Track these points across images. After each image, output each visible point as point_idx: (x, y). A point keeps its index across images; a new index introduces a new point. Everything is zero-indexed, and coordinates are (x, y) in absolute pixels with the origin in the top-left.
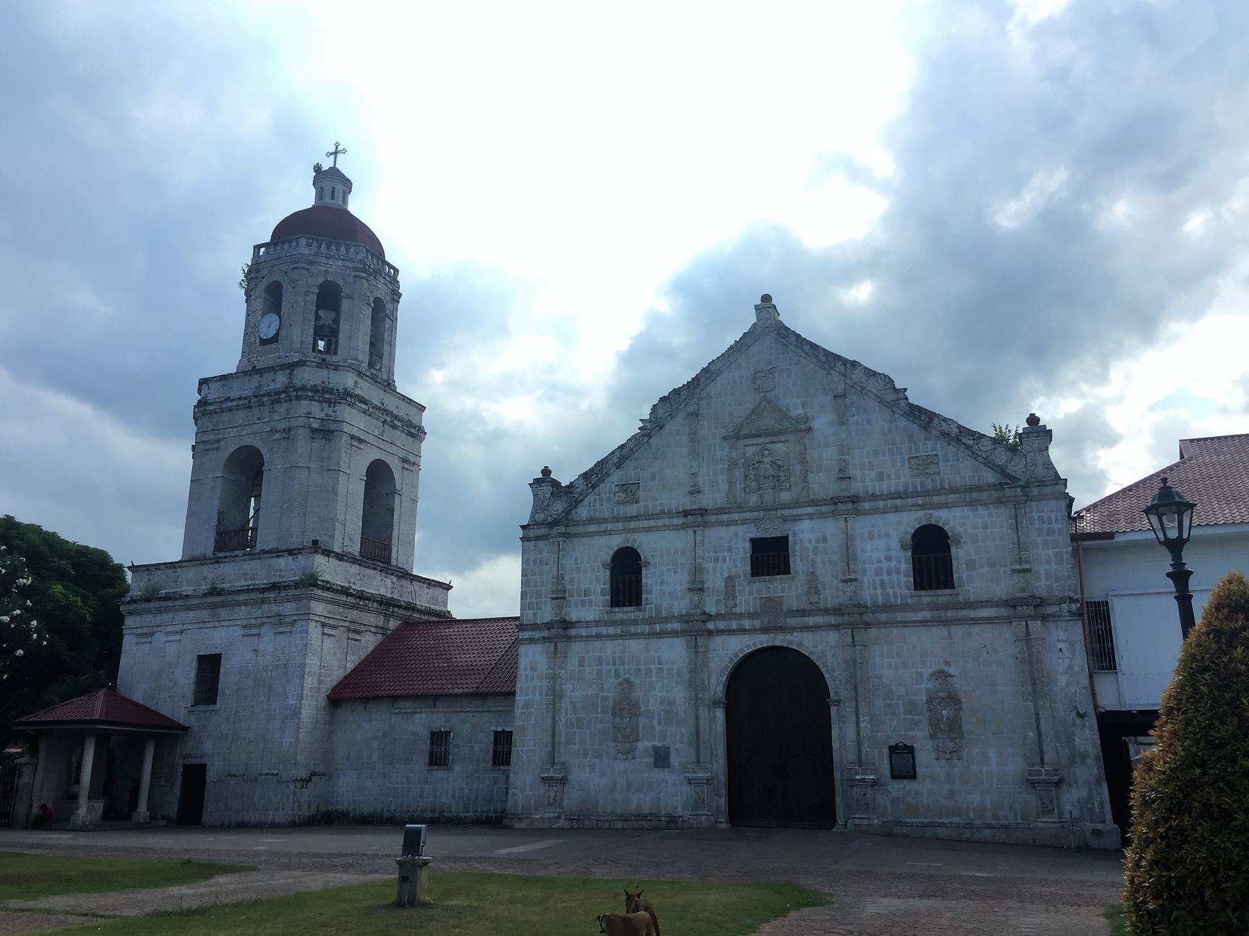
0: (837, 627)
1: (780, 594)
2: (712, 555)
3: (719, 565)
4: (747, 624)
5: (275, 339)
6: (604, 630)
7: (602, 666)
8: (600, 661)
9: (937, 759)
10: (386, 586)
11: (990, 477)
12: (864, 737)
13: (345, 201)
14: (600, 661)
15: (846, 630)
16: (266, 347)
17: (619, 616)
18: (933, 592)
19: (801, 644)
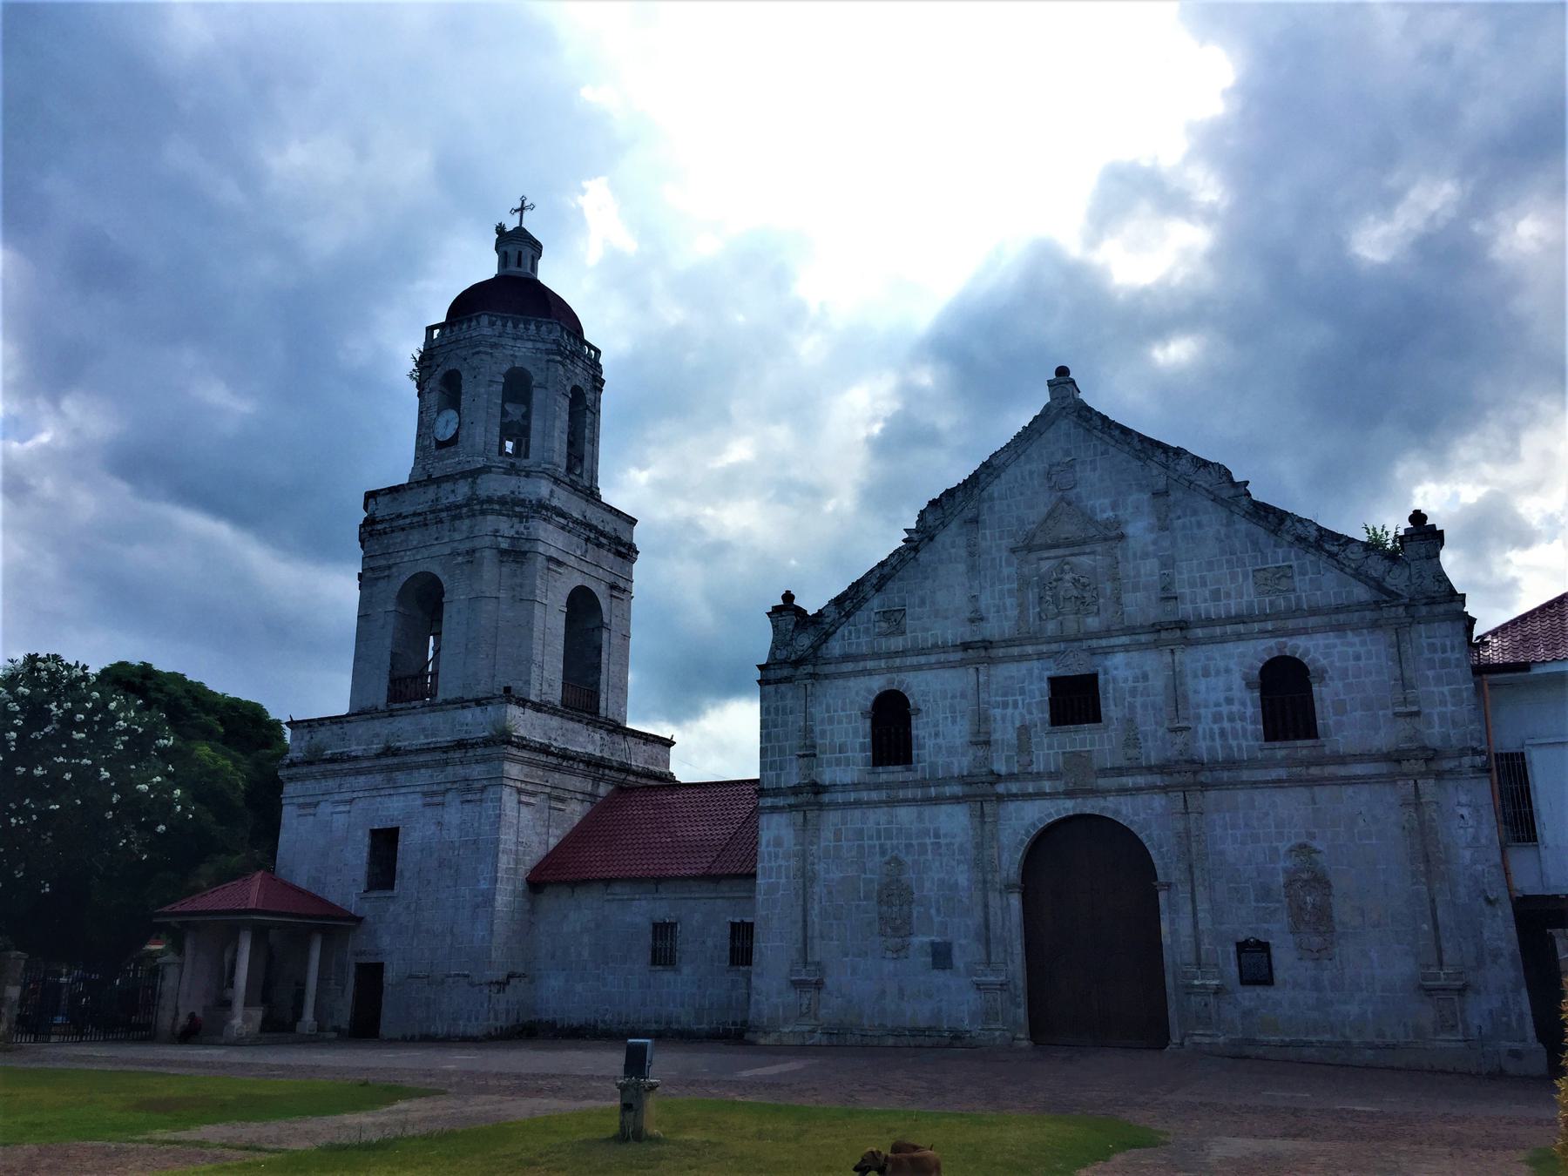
0: (1165, 789)
1: (1088, 748)
2: (999, 699)
3: (1010, 711)
4: (1047, 786)
5: (453, 441)
6: (865, 796)
7: (863, 840)
8: (860, 833)
9: (1300, 959)
10: (593, 742)
11: (1361, 592)
12: (1203, 932)
13: (534, 268)
14: (860, 833)
15: (1175, 794)
16: (443, 451)
17: (884, 777)
18: (1286, 743)
19: (1117, 812)
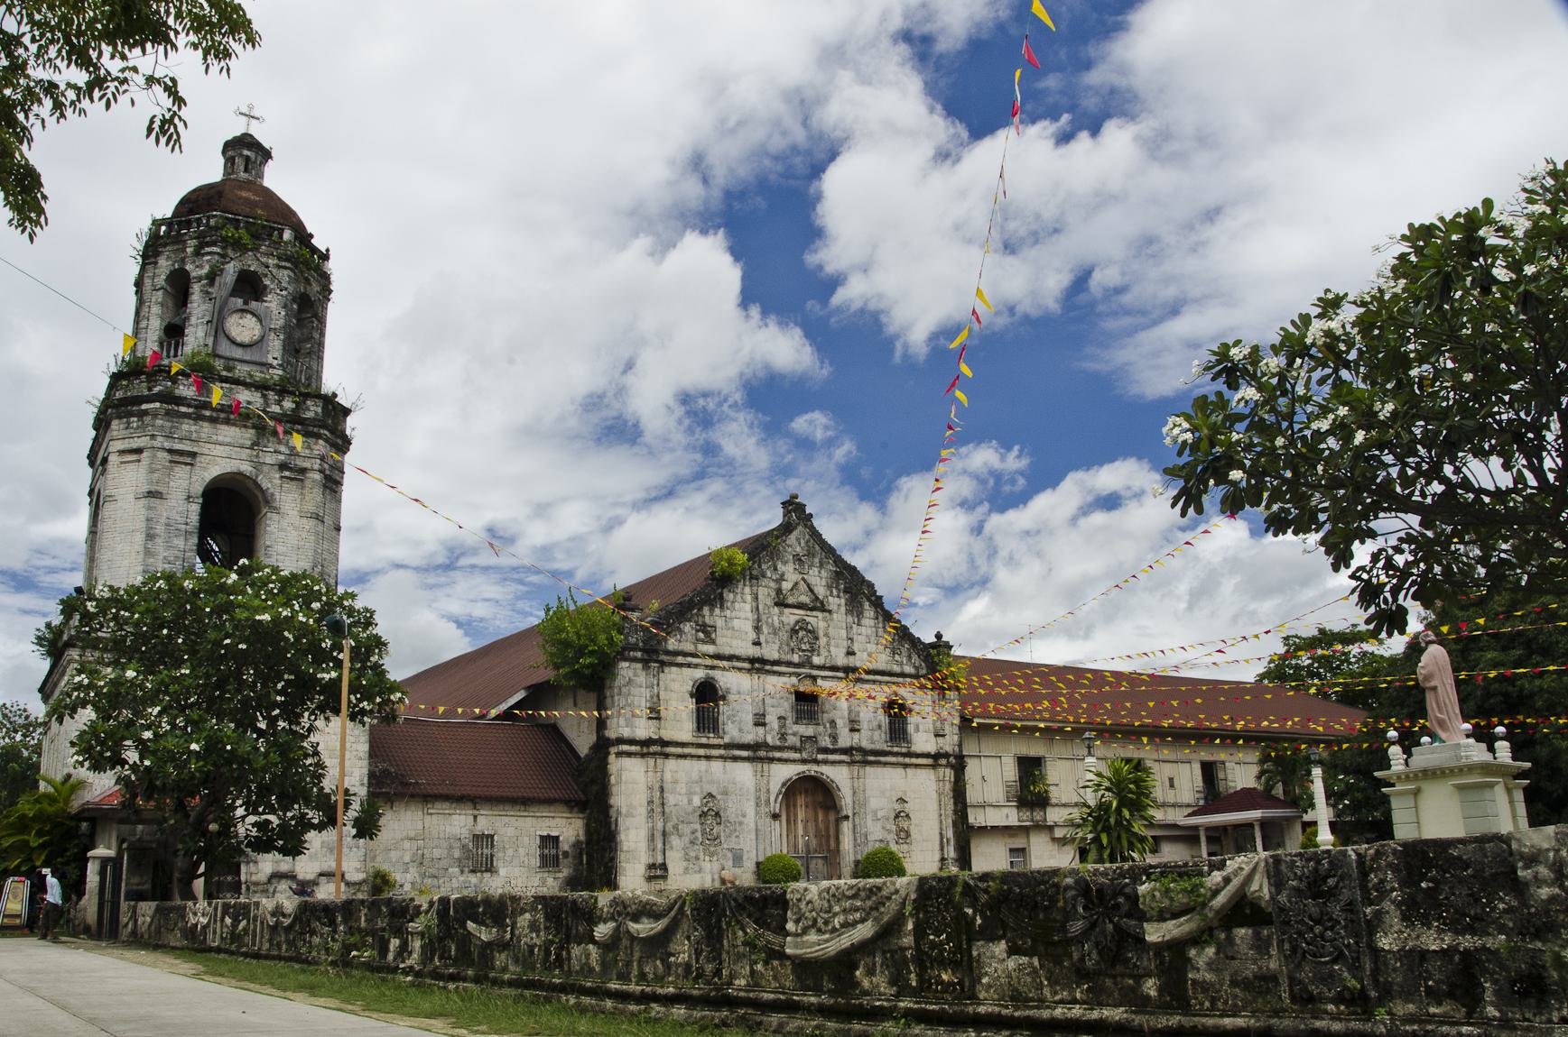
17: (704, 741)
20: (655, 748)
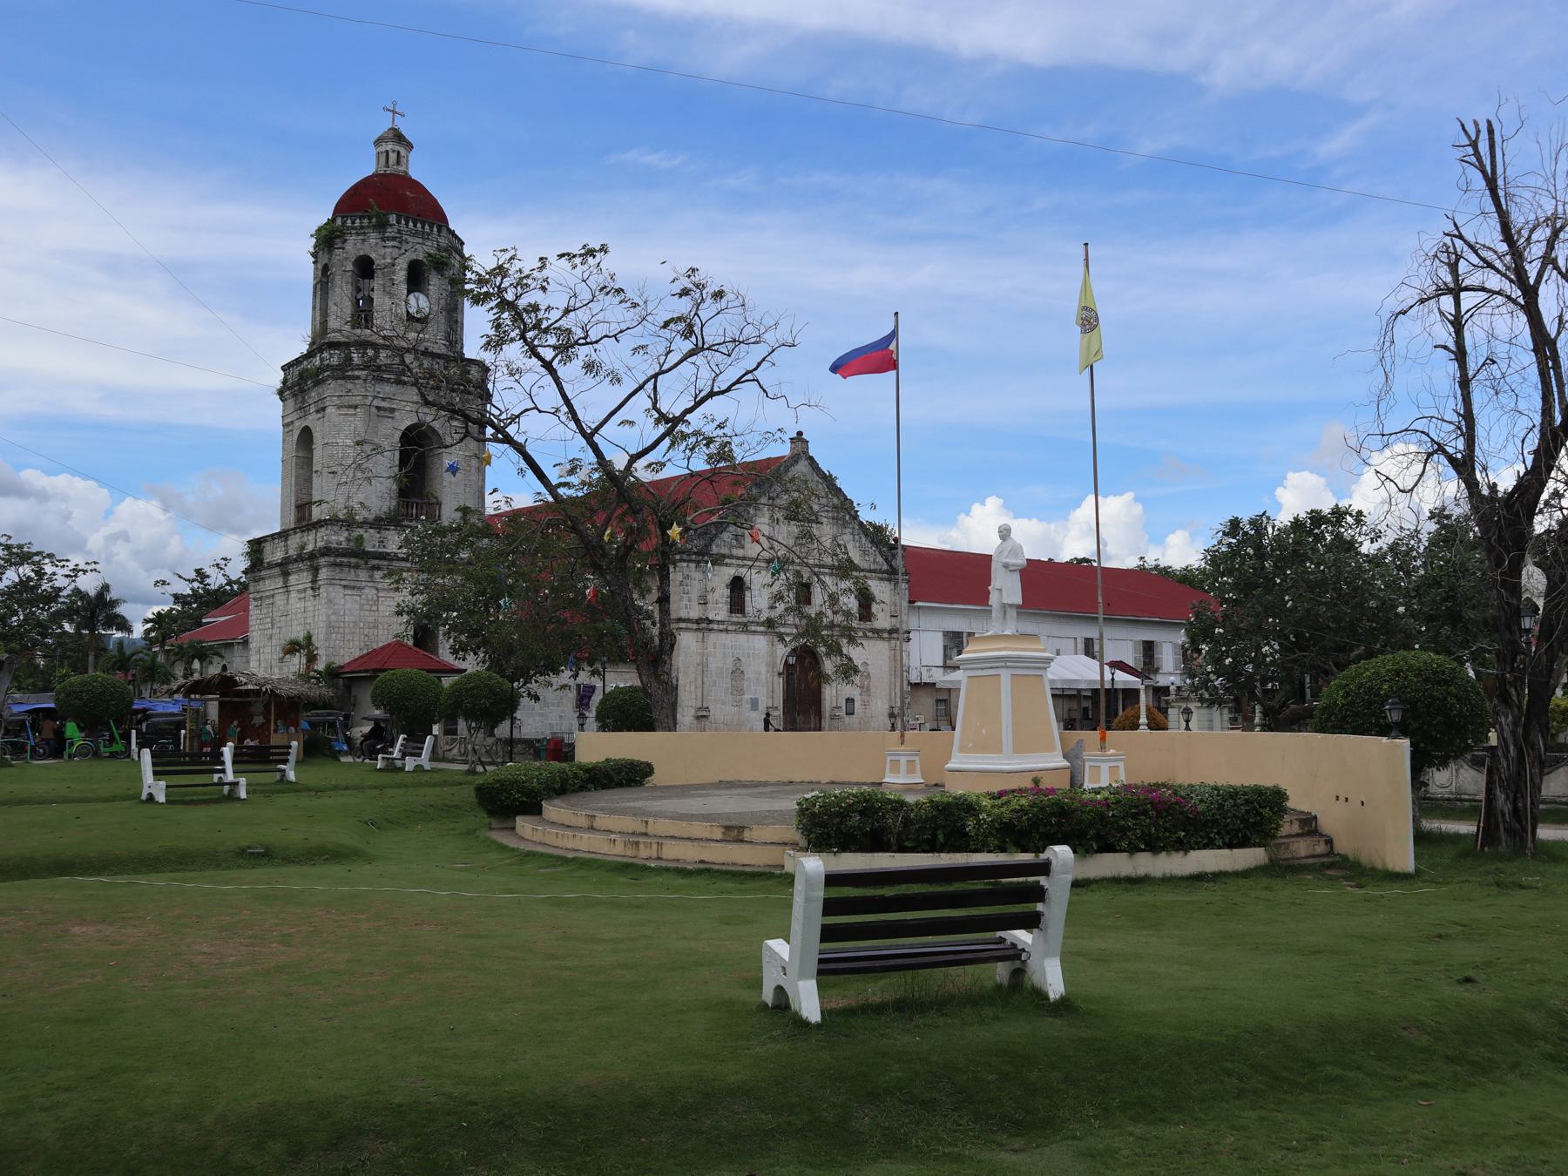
11: (885, 567)
17: (735, 619)
20: (704, 625)
